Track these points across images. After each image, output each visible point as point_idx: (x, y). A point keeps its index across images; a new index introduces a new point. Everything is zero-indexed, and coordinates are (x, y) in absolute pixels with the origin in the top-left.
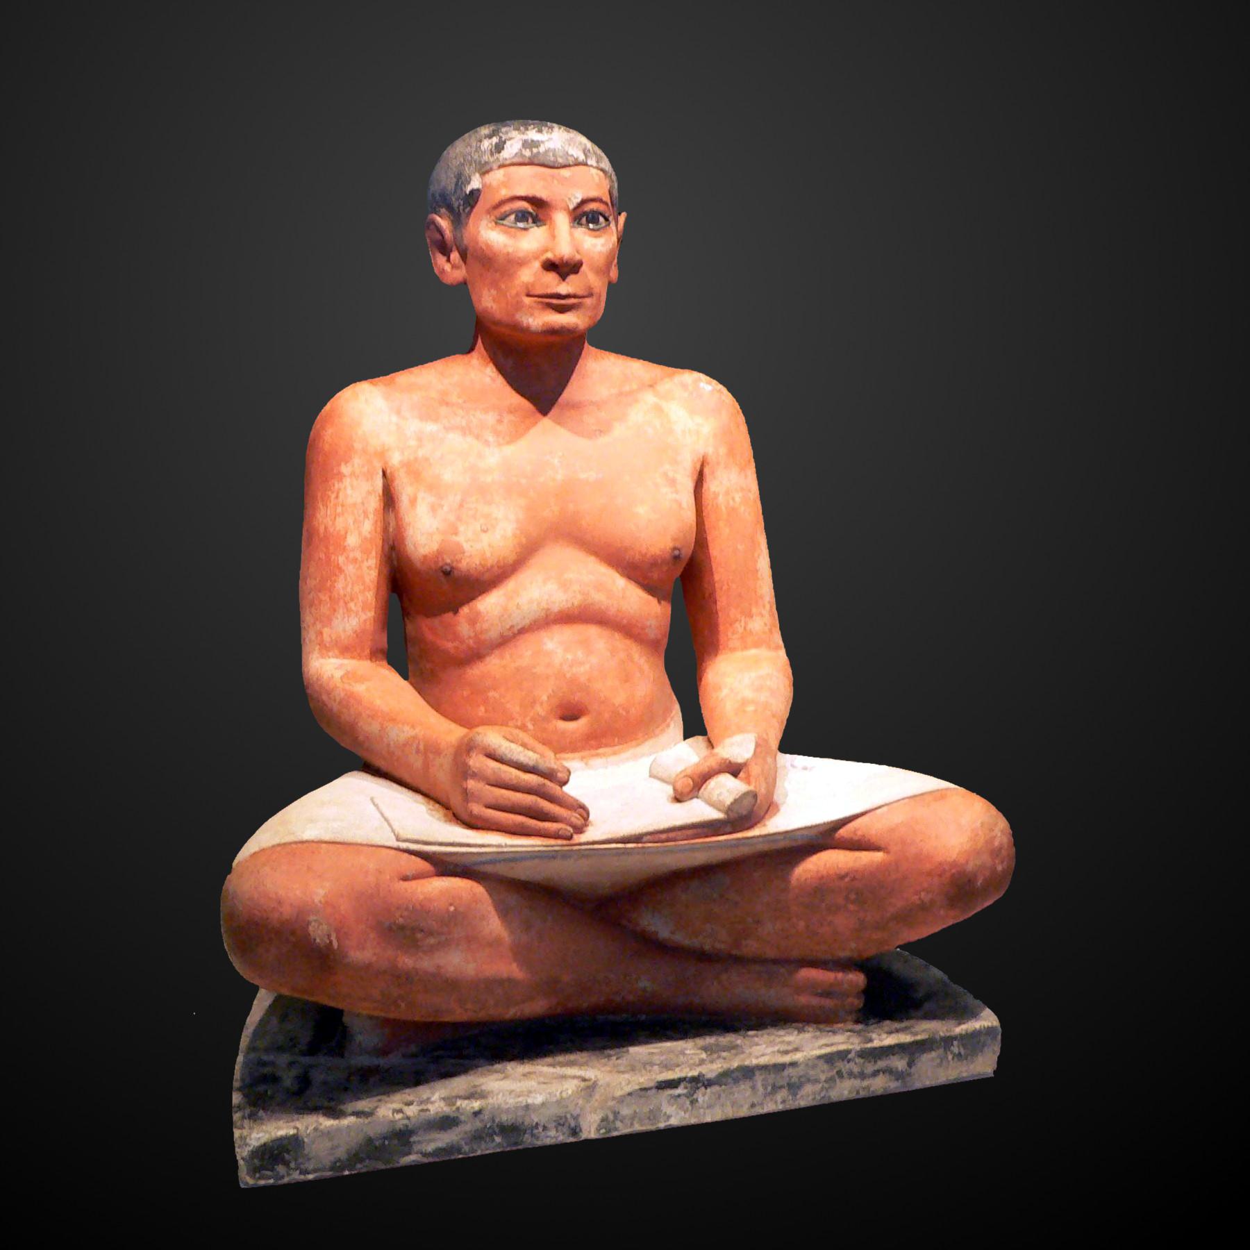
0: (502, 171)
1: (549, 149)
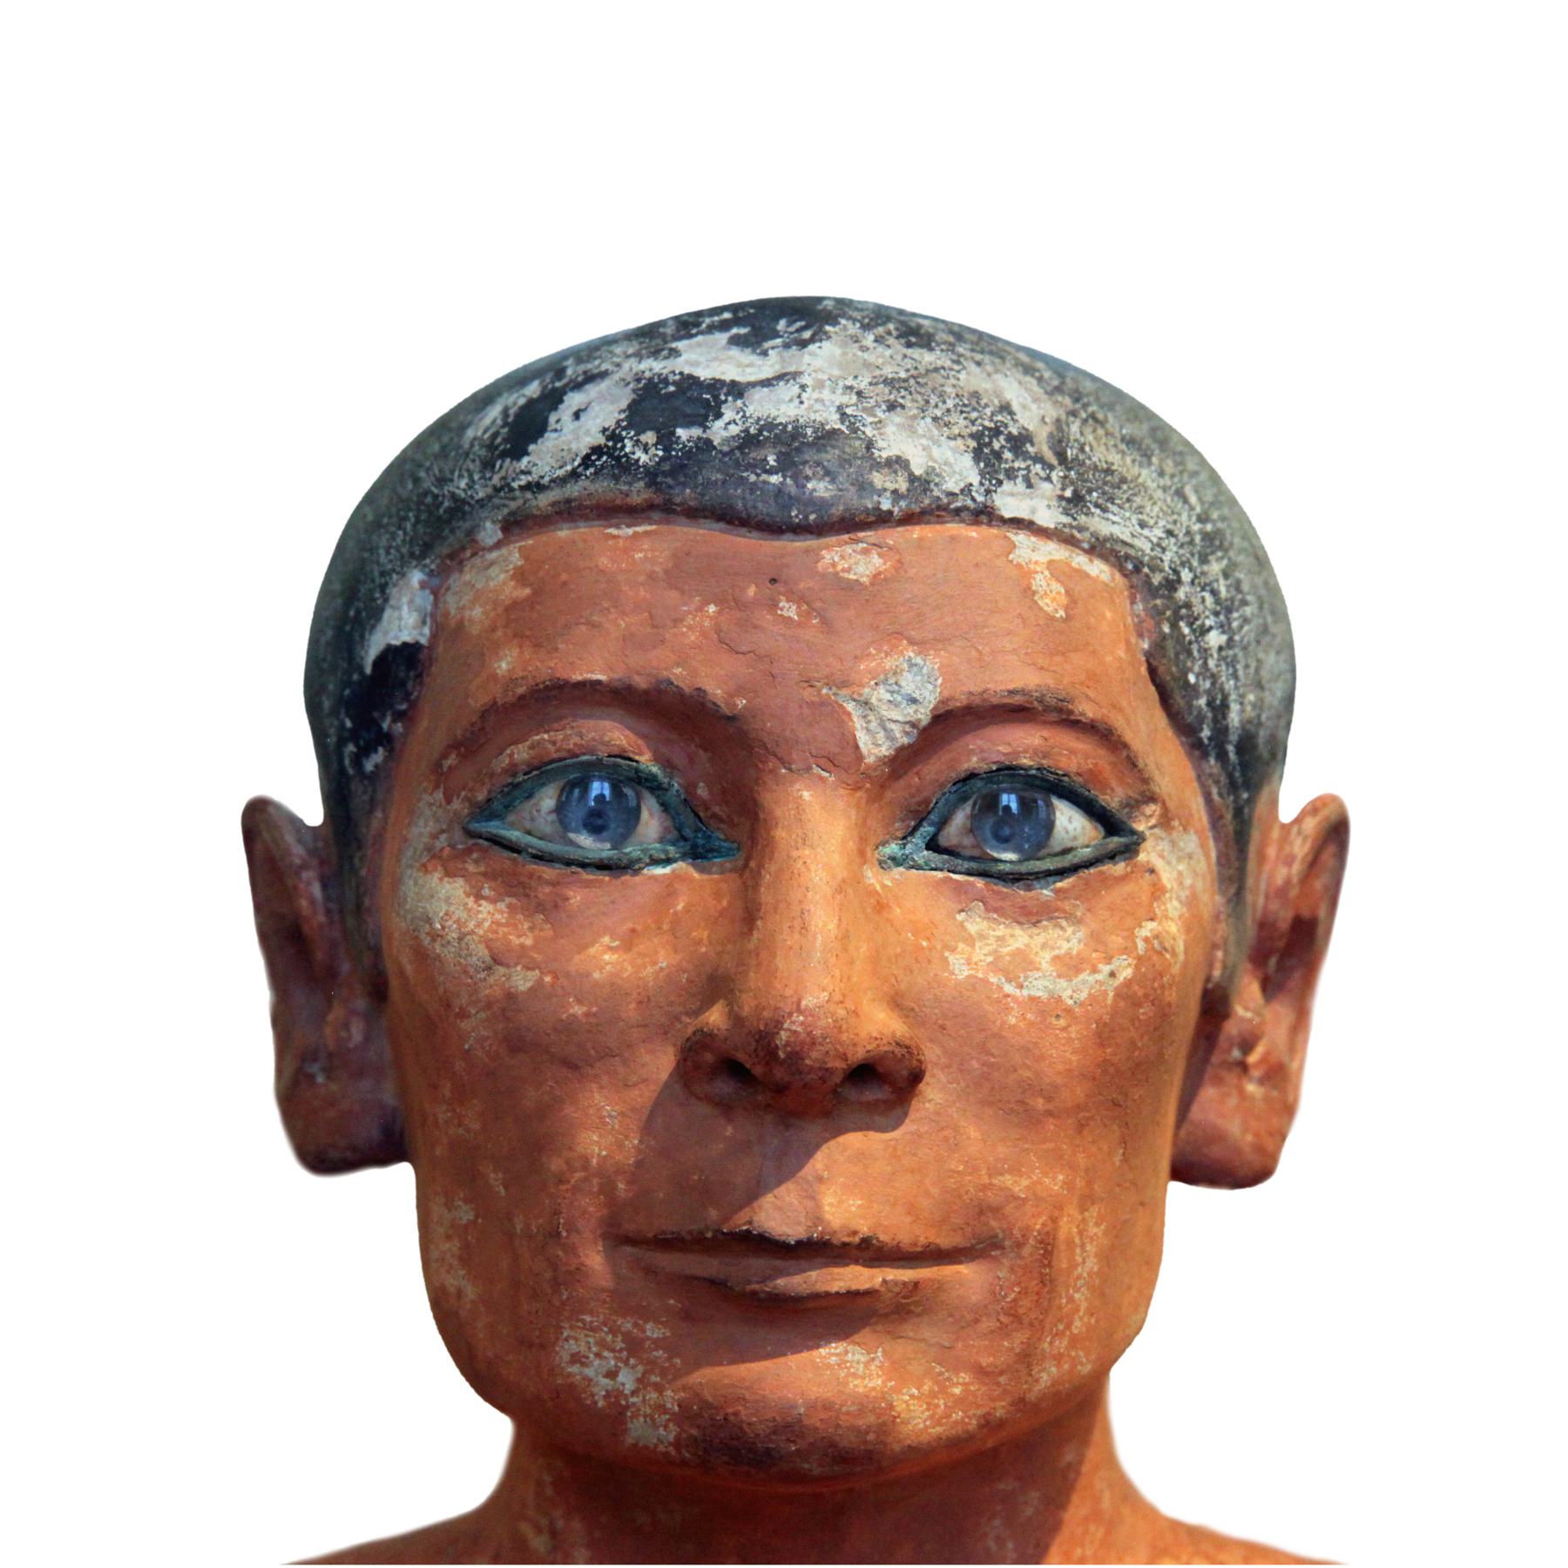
0: (513, 555)
1: (770, 425)
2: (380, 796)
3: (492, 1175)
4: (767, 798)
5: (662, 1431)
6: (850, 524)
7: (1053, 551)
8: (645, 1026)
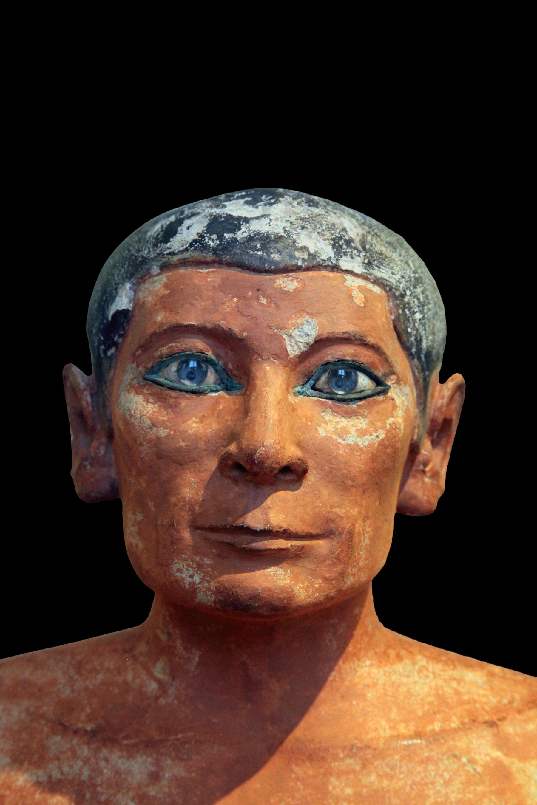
0: (164, 278)
1: (258, 233)
2: (113, 365)
3: (150, 503)
4: (253, 369)
5: (209, 597)
6: (286, 270)
7: (360, 282)
8: (207, 450)
